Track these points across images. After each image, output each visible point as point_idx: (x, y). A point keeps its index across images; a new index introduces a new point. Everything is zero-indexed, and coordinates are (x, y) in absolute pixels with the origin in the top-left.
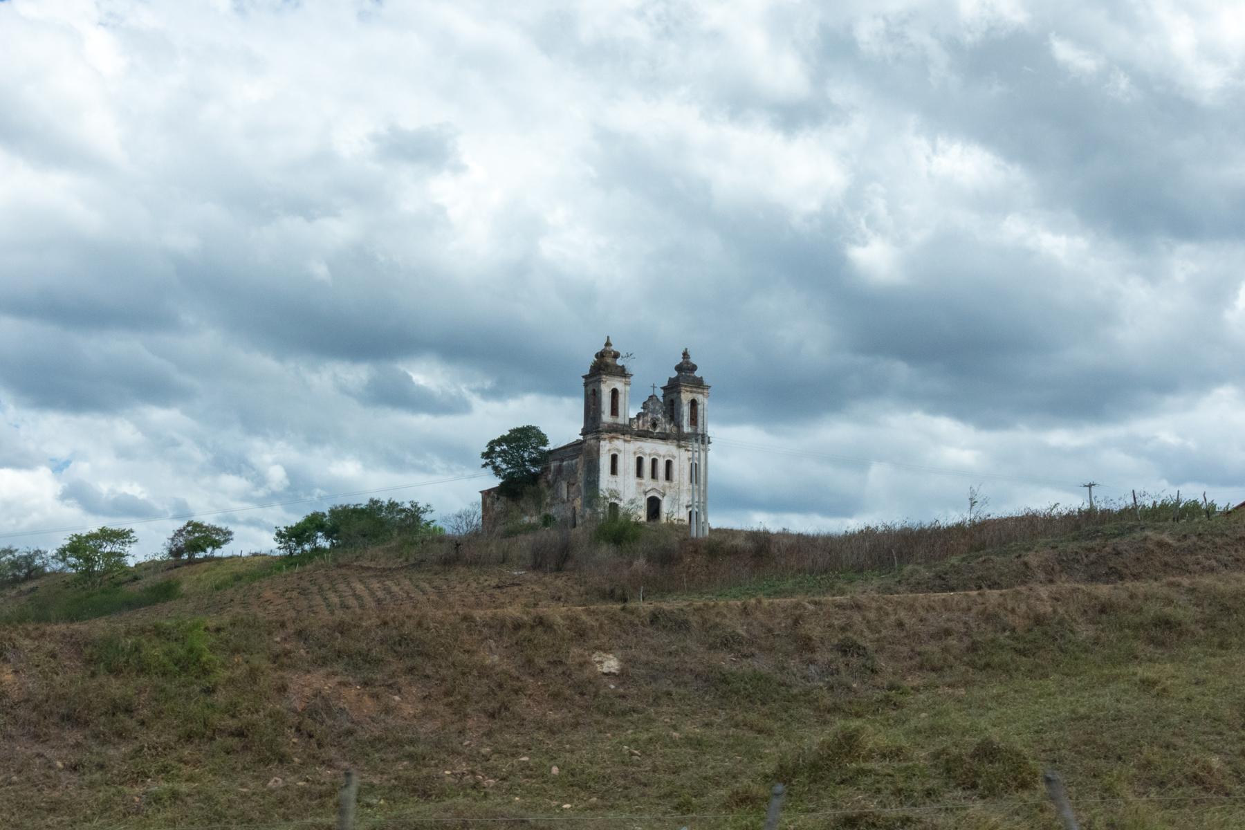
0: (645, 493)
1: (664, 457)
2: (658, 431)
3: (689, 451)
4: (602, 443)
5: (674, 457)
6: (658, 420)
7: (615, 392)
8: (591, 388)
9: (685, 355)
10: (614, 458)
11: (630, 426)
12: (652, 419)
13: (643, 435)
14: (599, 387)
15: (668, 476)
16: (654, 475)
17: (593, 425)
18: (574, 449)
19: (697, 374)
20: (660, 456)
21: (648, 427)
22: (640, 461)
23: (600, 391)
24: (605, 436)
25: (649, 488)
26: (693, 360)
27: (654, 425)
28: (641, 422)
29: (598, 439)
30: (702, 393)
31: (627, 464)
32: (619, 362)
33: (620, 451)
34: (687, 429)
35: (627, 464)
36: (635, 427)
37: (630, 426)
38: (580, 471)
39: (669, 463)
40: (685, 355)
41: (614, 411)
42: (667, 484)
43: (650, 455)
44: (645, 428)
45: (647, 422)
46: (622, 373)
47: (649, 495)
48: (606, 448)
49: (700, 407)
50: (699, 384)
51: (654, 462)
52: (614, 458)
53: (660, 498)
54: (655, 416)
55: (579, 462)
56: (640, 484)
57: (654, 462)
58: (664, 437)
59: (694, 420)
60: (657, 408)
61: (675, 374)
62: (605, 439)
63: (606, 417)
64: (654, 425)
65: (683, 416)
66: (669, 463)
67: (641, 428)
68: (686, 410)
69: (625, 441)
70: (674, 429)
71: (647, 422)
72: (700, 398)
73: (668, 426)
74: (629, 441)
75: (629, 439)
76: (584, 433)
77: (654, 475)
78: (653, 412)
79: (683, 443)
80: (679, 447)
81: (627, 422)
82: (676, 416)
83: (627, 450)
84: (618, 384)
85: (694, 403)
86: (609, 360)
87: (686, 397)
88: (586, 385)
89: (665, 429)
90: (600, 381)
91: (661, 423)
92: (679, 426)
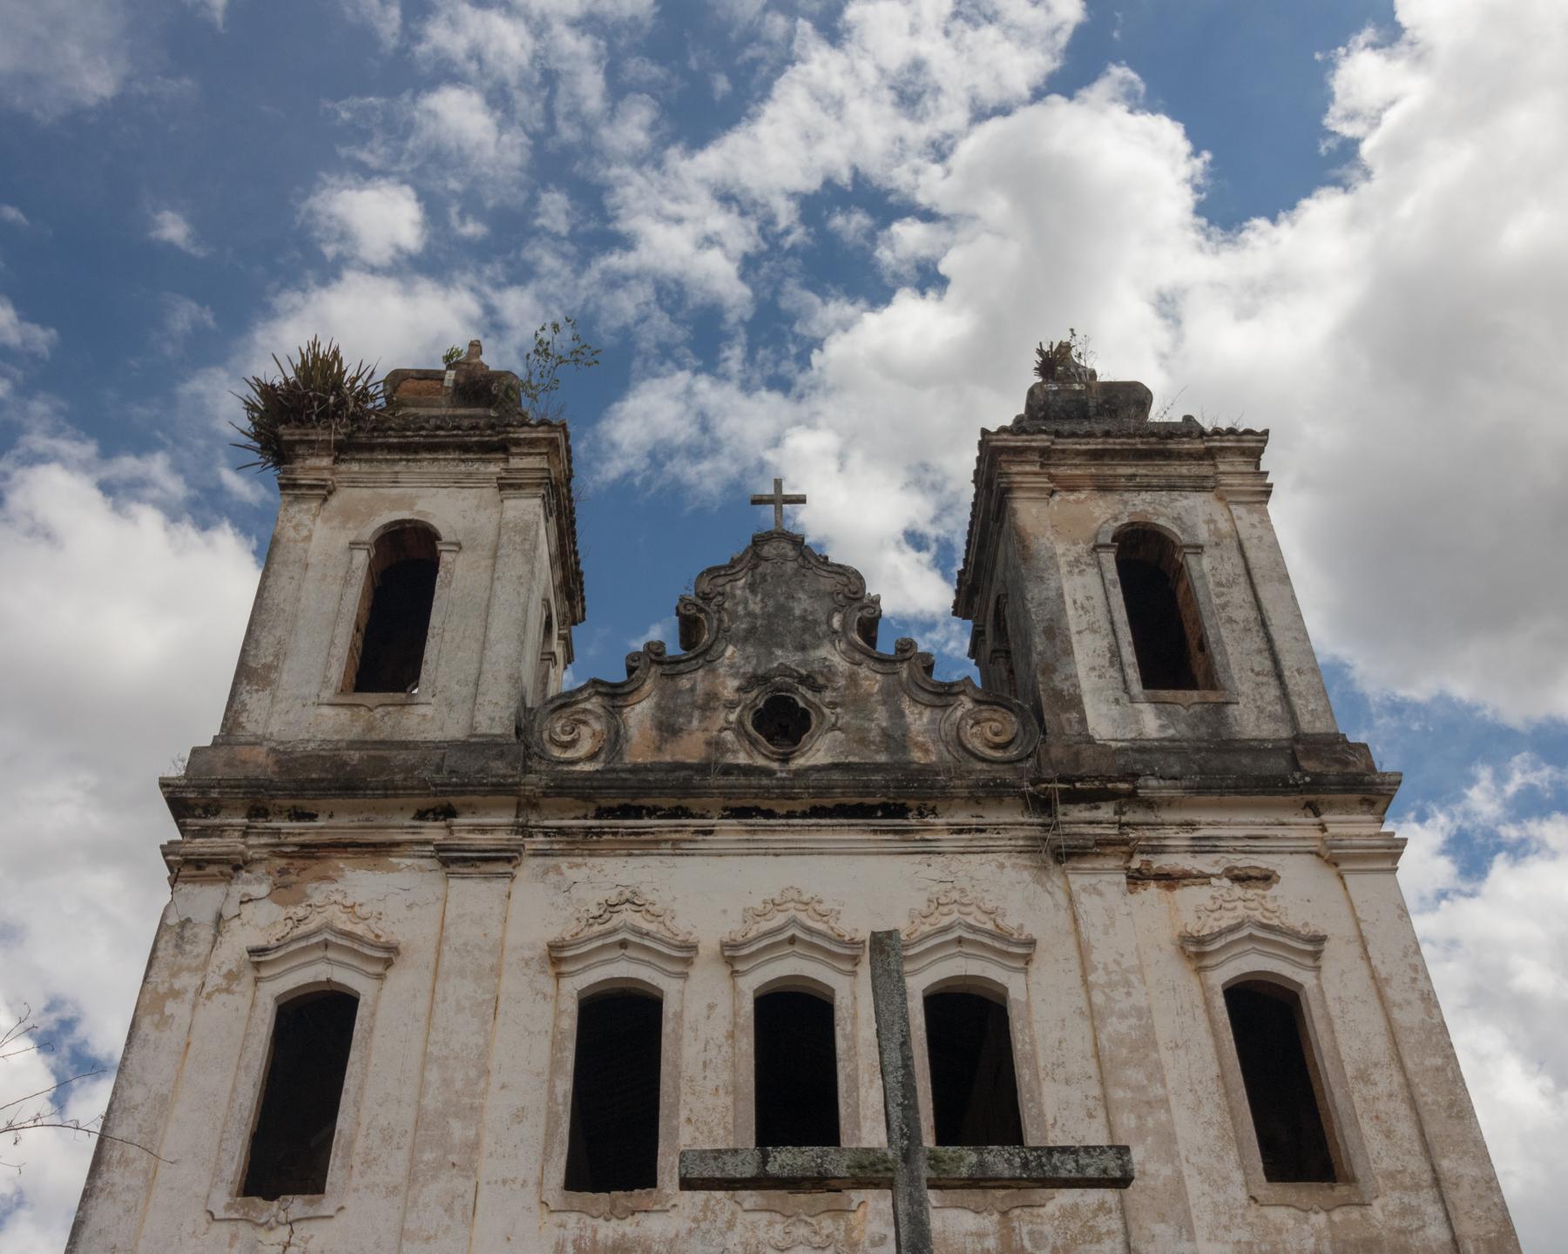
2: (818, 752)
3: (1170, 880)
5: (1023, 951)
12: (755, 681)
28: (639, 714)
43: (732, 956)
44: (690, 749)
45: (709, 703)
54: (785, 657)
60: (802, 604)
65: (1055, 631)
69: (452, 860)
71: (709, 703)
74: (499, 861)
75: (501, 838)
78: (762, 634)
79: (1080, 820)
89: (896, 739)
91: (859, 704)
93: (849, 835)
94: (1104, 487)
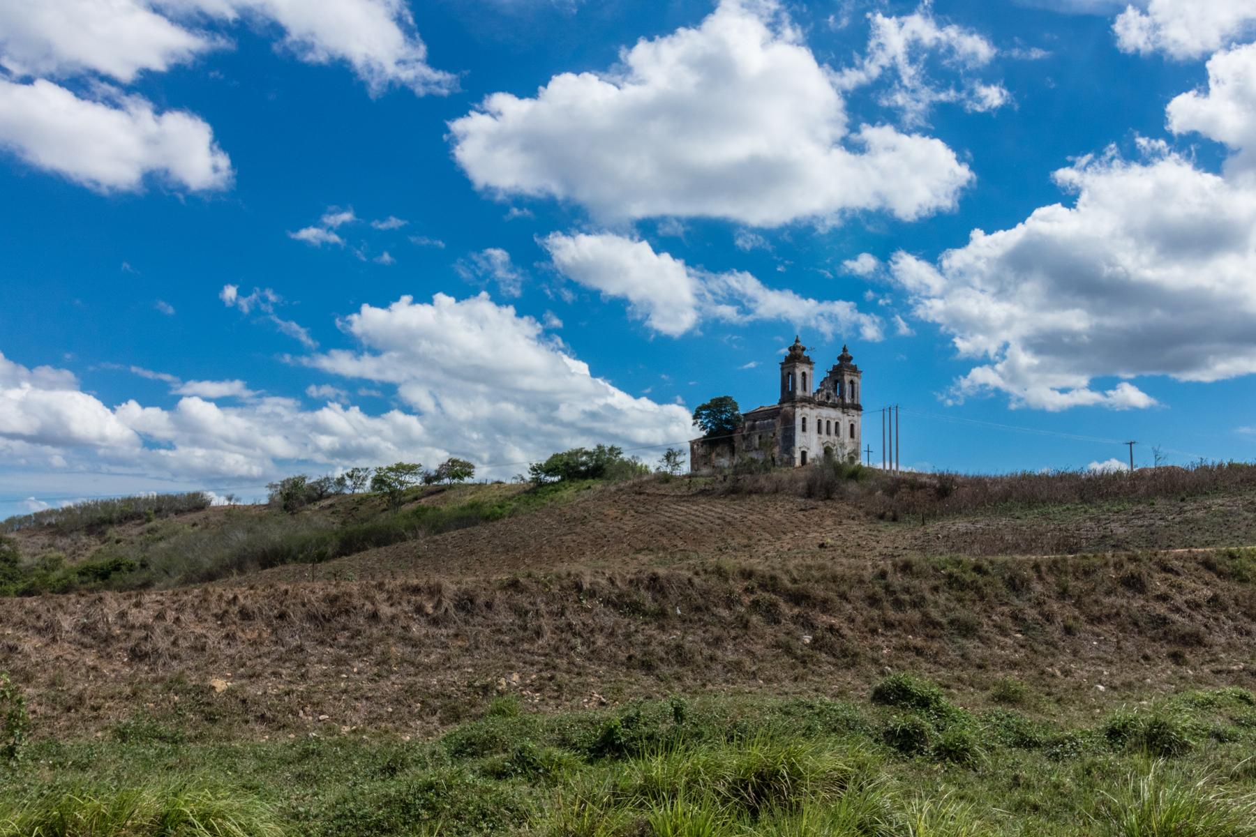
7: (804, 374)
8: (786, 371)
9: (845, 350)
10: (804, 420)
11: (813, 398)
13: (822, 404)
16: (828, 433)
17: (788, 396)
19: (852, 363)
21: (824, 399)
24: (799, 405)
26: (850, 354)
27: (828, 398)
29: (794, 407)
31: (812, 425)
32: (805, 354)
34: (848, 401)
35: (812, 425)
37: (813, 398)
39: (837, 424)
40: (845, 350)
41: (804, 389)
46: (808, 361)
48: (799, 413)
50: (854, 370)
51: (828, 422)
52: (804, 420)
57: (828, 422)
58: (834, 406)
61: (837, 363)
63: (799, 392)
64: (828, 398)
66: (837, 424)
72: (856, 379)
77: (828, 433)
80: (843, 412)
83: (811, 414)
84: (805, 368)
85: (852, 382)
86: (799, 351)
87: (847, 378)
88: (782, 369)
90: (794, 367)
92: (842, 397)
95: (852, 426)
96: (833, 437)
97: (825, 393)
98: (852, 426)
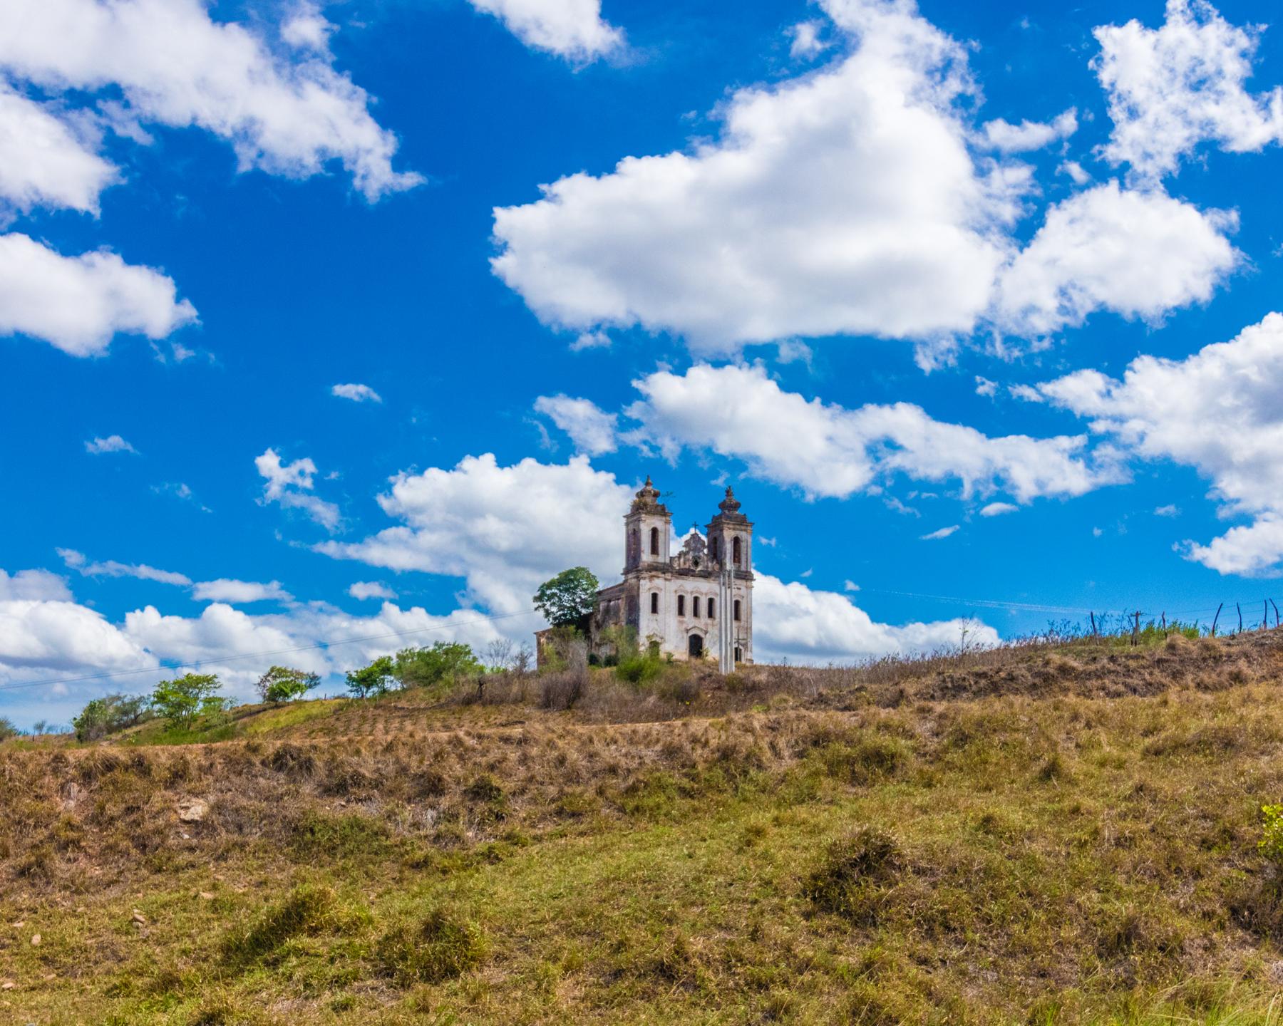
0: (687, 631)
1: (706, 594)
2: (700, 568)
4: (642, 582)
6: (699, 558)
7: (655, 532)
8: (631, 527)
10: (655, 596)
11: (671, 565)
13: (684, 573)
14: (639, 526)
15: (711, 614)
16: (696, 614)
17: (633, 564)
18: (621, 588)
20: (702, 594)
21: (689, 565)
22: (681, 599)
23: (640, 530)
24: (645, 575)
25: (691, 626)
27: (696, 563)
28: (682, 560)
29: (638, 578)
30: (745, 530)
31: (668, 602)
33: (658, 588)
35: (668, 602)
36: (676, 565)
37: (671, 565)
38: (622, 611)
39: (711, 601)
41: (654, 550)
42: (709, 621)
44: (687, 566)
47: (691, 633)
48: (646, 588)
49: (743, 544)
51: (696, 600)
52: (655, 596)
53: (702, 635)
55: (622, 603)
56: (681, 622)
57: (696, 600)
58: (706, 575)
59: (737, 557)
62: (645, 578)
63: (646, 557)
66: (711, 601)
67: (682, 566)
68: (729, 547)
69: (666, 579)
70: (717, 567)
72: (743, 535)
73: (710, 564)
74: (670, 580)
76: (626, 572)
81: (668, 561)
82: (719, 554)
83: (669, 589)
84: (657, 522)
85: (736, 541)
87: (728, 535)
88: (627, 524)
89: (707, 567)
90: (639, 520)
93: (701, 579)
94: (734, 529)
95: (737, 603)
96: (704, 618)
97: (690, 557)
98: (737, 603)
